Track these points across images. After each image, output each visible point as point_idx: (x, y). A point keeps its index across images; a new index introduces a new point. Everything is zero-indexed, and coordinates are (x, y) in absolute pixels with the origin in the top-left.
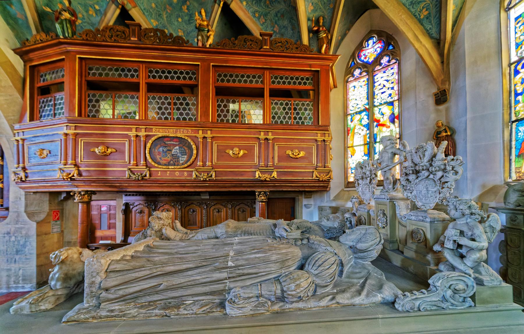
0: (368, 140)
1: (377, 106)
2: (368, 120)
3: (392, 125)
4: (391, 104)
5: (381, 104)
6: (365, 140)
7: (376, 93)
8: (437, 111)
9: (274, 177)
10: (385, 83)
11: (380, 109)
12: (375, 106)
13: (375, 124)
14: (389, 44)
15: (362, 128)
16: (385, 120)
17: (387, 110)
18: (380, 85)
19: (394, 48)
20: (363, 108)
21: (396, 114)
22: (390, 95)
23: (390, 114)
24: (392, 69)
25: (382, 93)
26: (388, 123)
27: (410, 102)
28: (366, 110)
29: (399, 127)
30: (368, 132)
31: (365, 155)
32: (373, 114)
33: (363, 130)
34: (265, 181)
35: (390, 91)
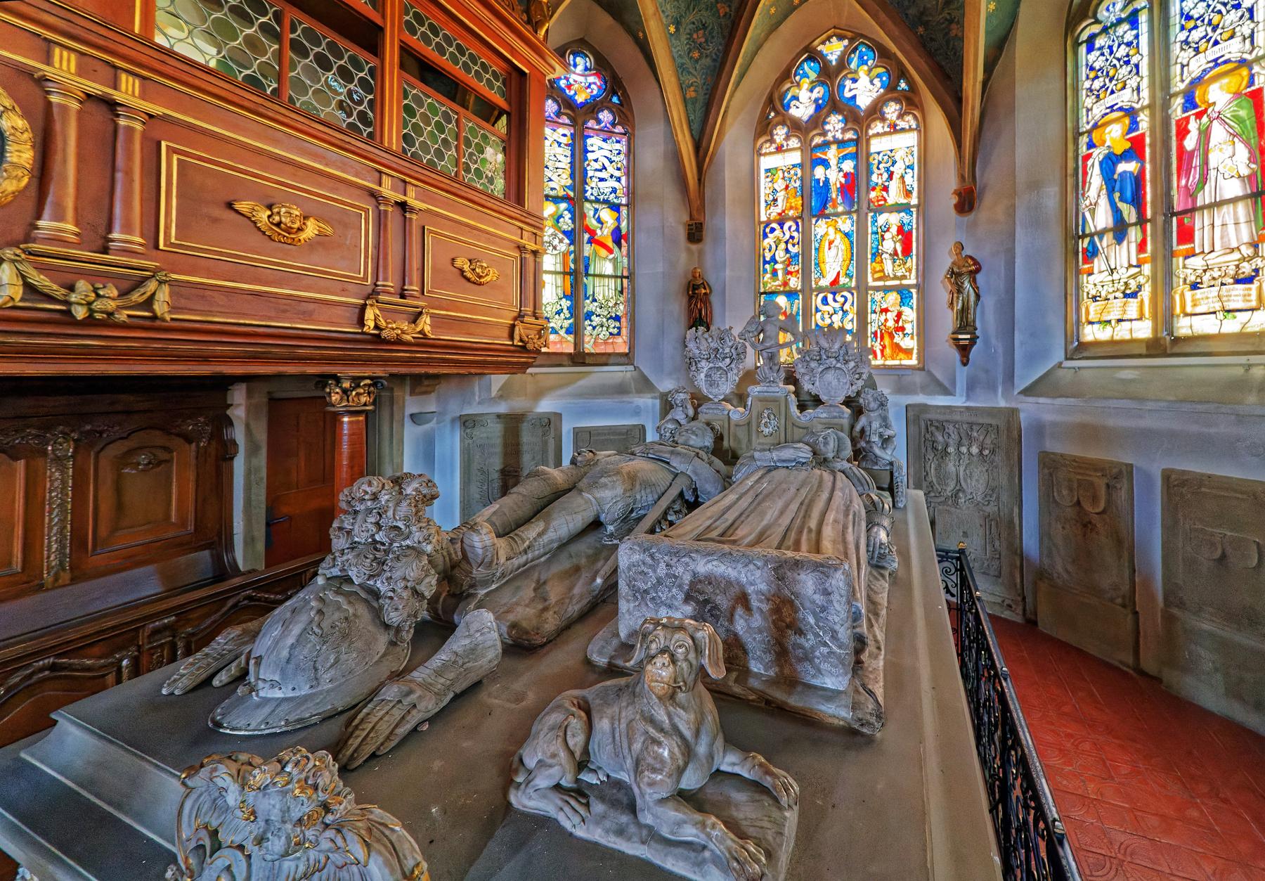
0: (572, 266)
1: (591, 202)
2: (574, 222)
3: (616, 249)
4: (616, 208)
5: (597, 201)
6: (565, 264)
7: (590, 174)
8: (689, 250)
9: (421, 332)
10: (607, 163)
11: (596, 210)
12: (587, 200)
13: (587, 236)
14: (615, 93)
15: (561, 236)
16: (605, 234)
17: (607, 215)
18: (596, 161)
19: (621, 104)
20: (561, 193)
21: (624, 232)
22: (614, 191)
23: (613, 227)
24: (618, 142)
25: (601, 180)
26: (610, 244)
27: (650, 218)
28: (566, 198)
29: (628, 255)
30: (572, 248)
31: (565, 296)
32: (583, 216)
33: (561, 241)
34: (398, 341)
35: (616, 185)
